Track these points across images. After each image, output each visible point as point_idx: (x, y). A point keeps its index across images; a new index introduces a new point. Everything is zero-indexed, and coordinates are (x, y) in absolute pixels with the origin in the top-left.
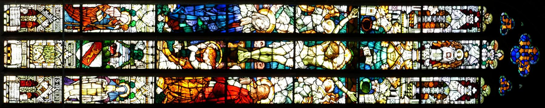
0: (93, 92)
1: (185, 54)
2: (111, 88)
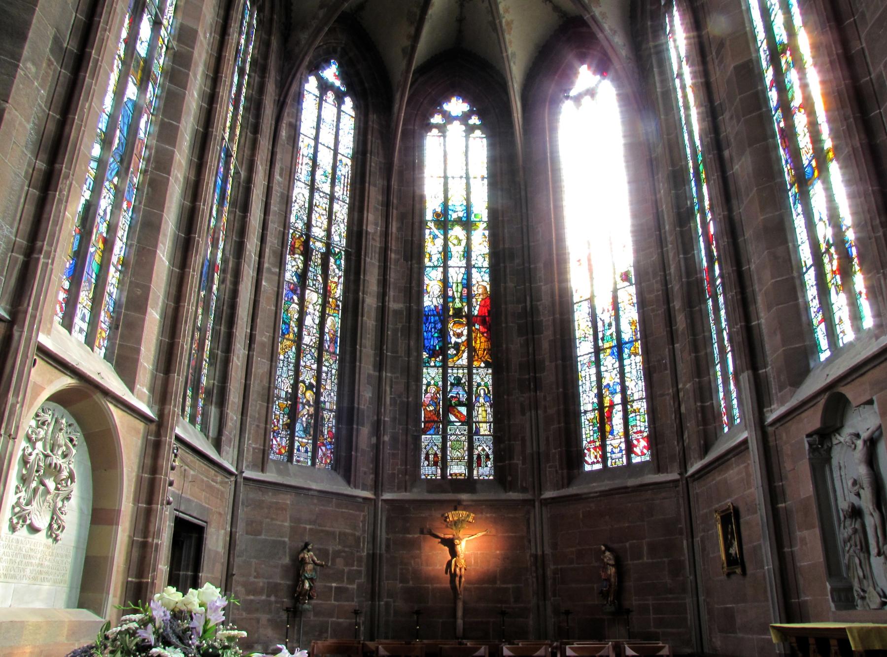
0: (484, 413)
1: (457, 346)
2: (482, 400)
